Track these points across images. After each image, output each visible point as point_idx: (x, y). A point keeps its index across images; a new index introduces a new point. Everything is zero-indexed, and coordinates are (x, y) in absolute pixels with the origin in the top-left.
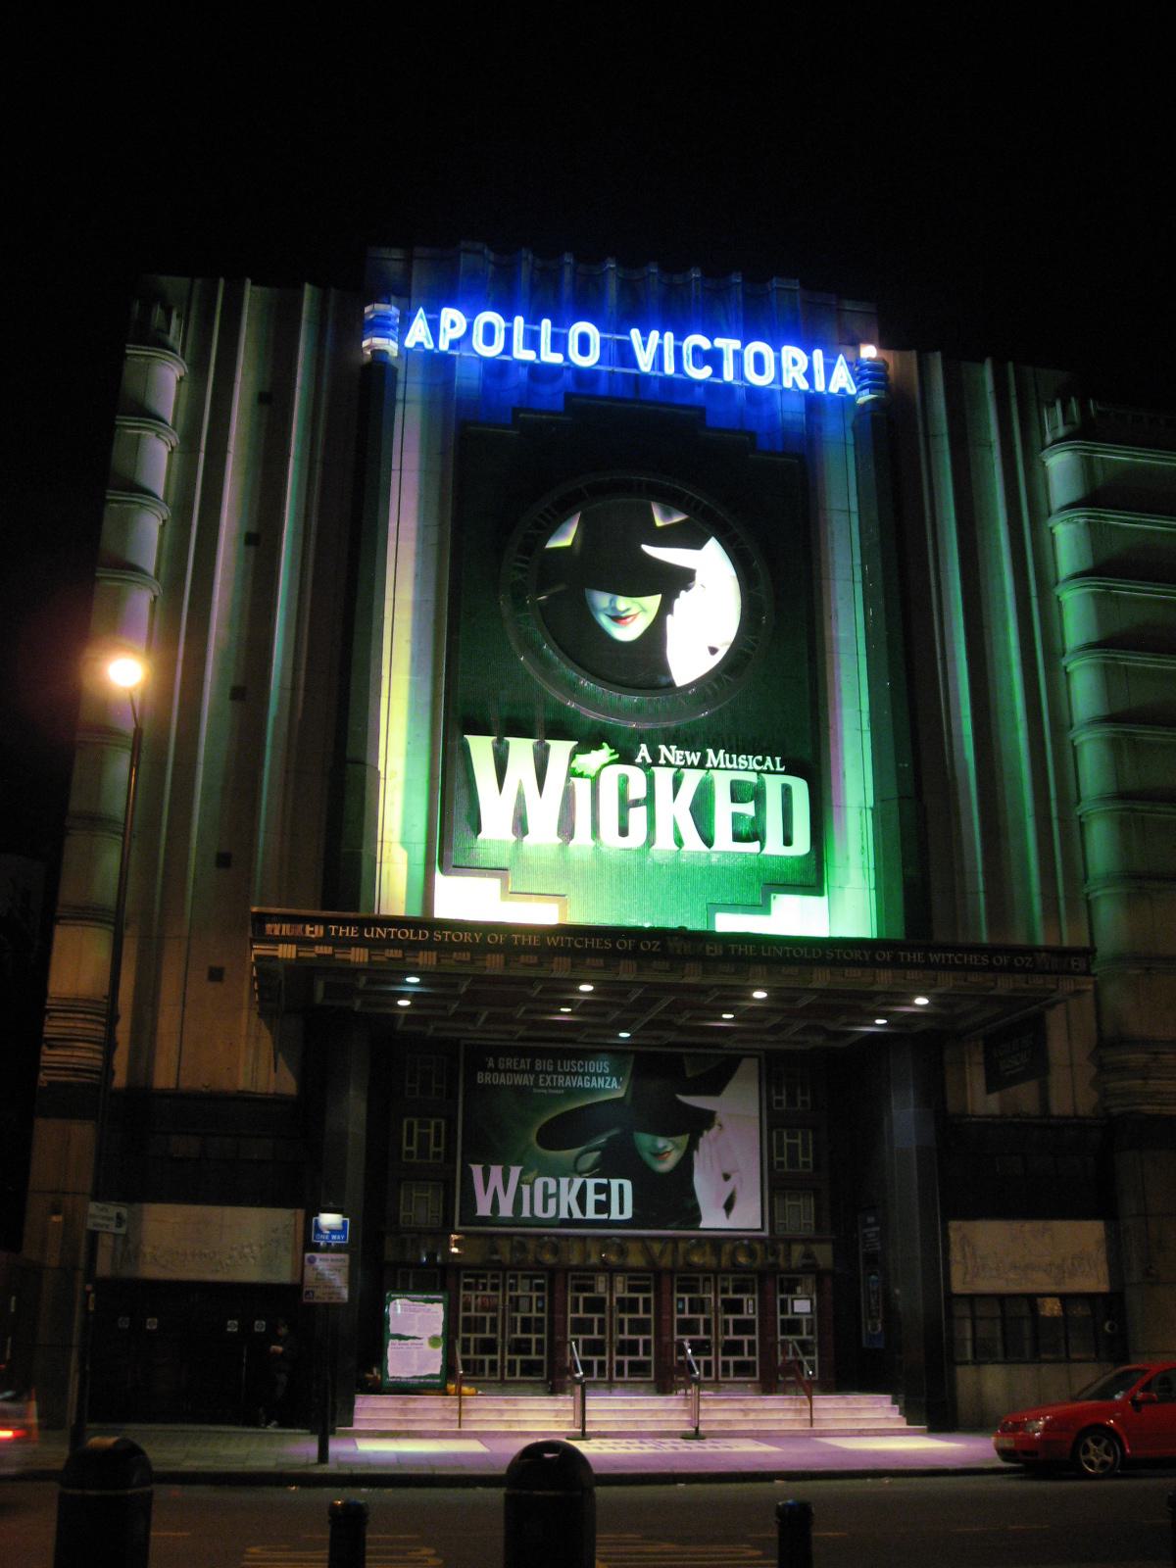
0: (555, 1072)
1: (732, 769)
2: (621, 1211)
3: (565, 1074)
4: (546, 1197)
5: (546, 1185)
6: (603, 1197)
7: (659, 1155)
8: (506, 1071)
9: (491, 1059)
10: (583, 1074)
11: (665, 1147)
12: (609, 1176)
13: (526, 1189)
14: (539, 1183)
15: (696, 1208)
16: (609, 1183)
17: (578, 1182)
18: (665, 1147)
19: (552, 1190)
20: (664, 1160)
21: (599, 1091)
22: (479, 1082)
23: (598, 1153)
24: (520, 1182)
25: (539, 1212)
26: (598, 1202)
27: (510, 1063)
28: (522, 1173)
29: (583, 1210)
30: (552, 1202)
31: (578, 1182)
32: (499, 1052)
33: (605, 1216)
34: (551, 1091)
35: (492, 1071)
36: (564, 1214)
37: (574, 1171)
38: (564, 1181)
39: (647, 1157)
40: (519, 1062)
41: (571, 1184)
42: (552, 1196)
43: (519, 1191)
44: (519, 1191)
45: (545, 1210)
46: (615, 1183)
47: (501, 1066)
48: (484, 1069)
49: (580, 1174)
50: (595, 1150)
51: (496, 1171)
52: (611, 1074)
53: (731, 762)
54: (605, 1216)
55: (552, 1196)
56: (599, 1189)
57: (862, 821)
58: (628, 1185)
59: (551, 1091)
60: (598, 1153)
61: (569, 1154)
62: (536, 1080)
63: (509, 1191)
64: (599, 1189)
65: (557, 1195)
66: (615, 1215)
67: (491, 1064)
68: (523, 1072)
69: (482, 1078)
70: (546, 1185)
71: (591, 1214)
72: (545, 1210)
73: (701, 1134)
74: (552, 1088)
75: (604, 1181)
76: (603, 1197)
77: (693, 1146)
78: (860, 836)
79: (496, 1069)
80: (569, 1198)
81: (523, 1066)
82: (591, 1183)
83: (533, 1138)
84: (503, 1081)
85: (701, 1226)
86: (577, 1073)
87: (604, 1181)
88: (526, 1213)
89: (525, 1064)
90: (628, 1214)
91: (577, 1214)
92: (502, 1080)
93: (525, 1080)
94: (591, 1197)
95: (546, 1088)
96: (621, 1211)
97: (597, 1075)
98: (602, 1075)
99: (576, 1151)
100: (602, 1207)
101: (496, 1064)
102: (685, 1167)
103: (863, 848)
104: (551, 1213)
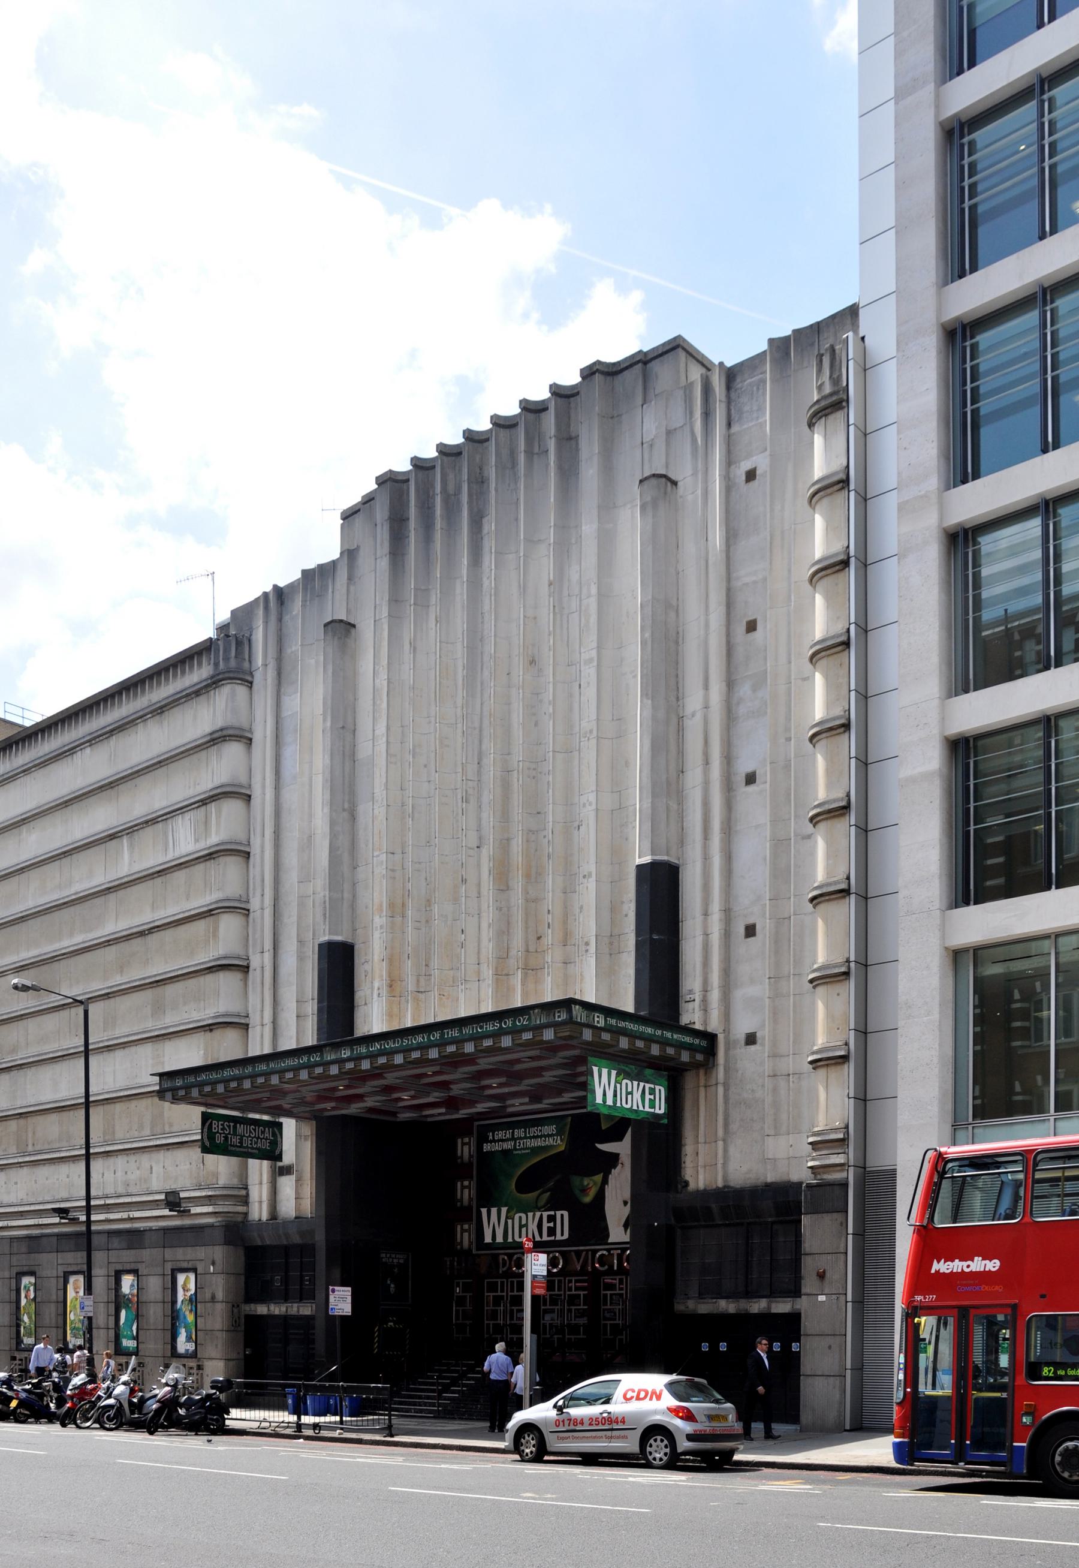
0: (526, 1137)
2: (562, 1235)
3: (531, 1138)
4: (521, 1227)
5: (520, 1218)
6: (551, 1225)
7: (584, 1190)
8: (499, 1141)
10: (541, 1137)
11: (588, 1184)
12: (556, 1209)
13: (510, 1221)
15: (606, 1229)
17: (538, 1214)
18: (588, 1184)
19: (524, 1222)
20: (587, 1195)
21: (551, 1147)
23: (549, 1193)
24: (507, 1218)
26: (549, 1228)
27: (500, 1135)
28: (508, 1212)
29: (541, 1236)
31: (538, 1214)
34: (523, 1152)
35: (491, 1142)
37: (535, 1208)
38: (530, 1215)
39: (577, 1192)
43: (506, 1223)
44: (506, 1223)
46: (559, 1213)
48: (487, 1141)
50: (546, 1192)
51: (494, 1210)
52: (556, 1135)
58: (566, 1214)
59: (523, 1152)
60: (549, 1193)
61: (532, 1196)
62: (515, 1144)
65: (526, 1225)
66: (559, 1237)
67: (491, 1138)
69: (487, 1147)
70: (520, 1218)
71: (545, 1238)
73: (610, 1173)
74: (524, 1149)
75: (552, 1213)
76: (551, 1225)
77: (605, 1181)
79: (494, 1141)
81: (508, 1136)
82: (545, 1214)
83: (513, 1186)
85: (610, 1241)
86: (538, 1137)
87: (552, 1213)
88: (510, 1240)
90: (566, 1236)
91: (538, 1238)
93: (509, 1145)
94: (546, 1225)
95: (521, 1149)
96: (562, 1235)
97: (549, 1136)
98: (552, 1135)
99: (535, 1194)
100: (552, 1231)
102: (600, 1197)
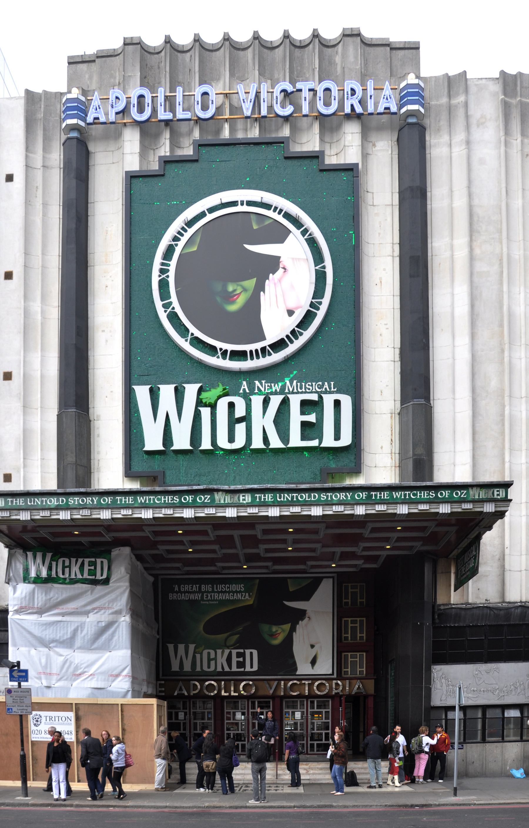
1: (302, 393)
4: (209, 660)
5: (209, 654)
6: (241, 659)
9: (176, 586)
14: (205, 652)
16: (244, 651)
17: (227, 652)
19: (212, 656)
22: (170, 599)
25: (205, 668)
30: (213, 663)
31: (227, 652)
32: (180, 582)
33: (242, 670)
36: (219, 669)
37: (224, 645)
38: (219, 652)
40: (192, 587)
41: (223, 653)
42: (212, 659)
45: (209, 667)
47: (182, 590)
49: (228, 647)
53: (301, 388)
54: (242, 670)
55: (212, 659)
56: (239, 655)
57: (392, 423)
61: (222, 637)
63: (188, 658)
64: (239, 655)
65: (215, 659)
68: (194, 592)
70: (209, 654)
71: (234, 669)
72: (209, 667)
75: (242, 651)
76: (241, 659)
78: (390, 432)
80: (222, 660)
81: (194, 589)
82: (234, 652)
84: (183, 598)
89: (195, 588)
91: (227, 669)
92: (183, 597)
94: (234, 660)
99: (225, 635)
101: (179, 589)
103: (392, 440)
104: (212, 668)
